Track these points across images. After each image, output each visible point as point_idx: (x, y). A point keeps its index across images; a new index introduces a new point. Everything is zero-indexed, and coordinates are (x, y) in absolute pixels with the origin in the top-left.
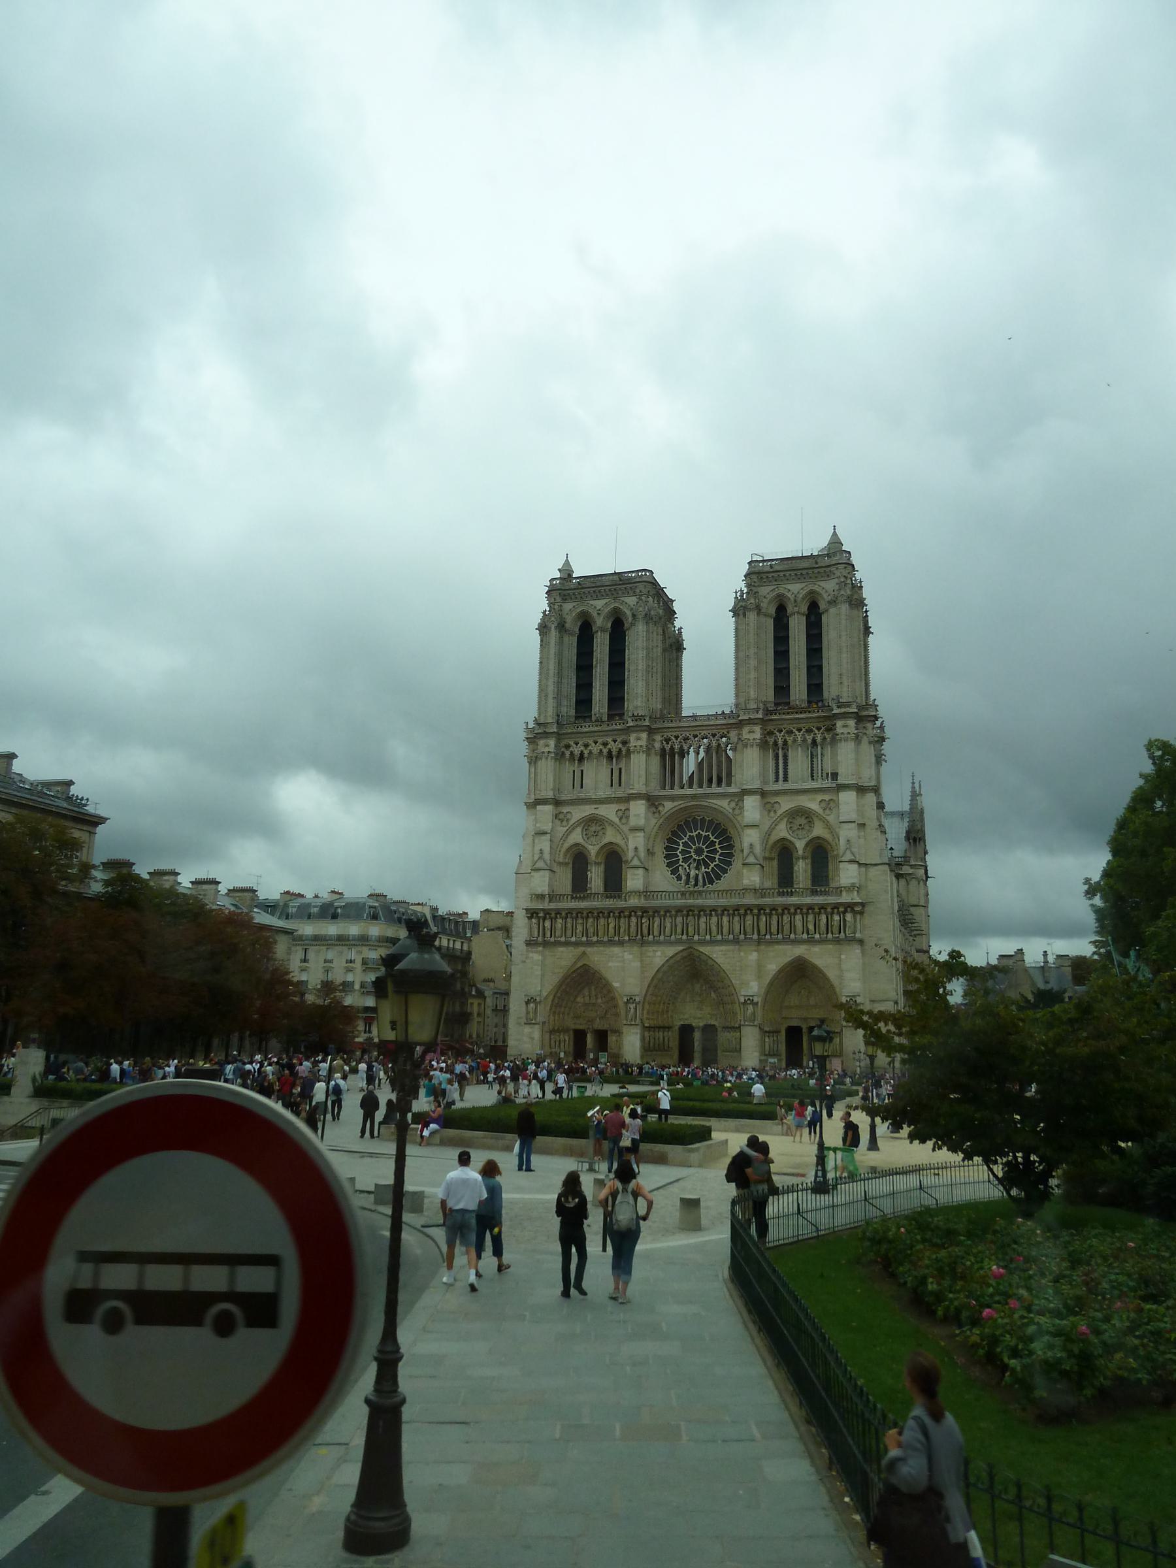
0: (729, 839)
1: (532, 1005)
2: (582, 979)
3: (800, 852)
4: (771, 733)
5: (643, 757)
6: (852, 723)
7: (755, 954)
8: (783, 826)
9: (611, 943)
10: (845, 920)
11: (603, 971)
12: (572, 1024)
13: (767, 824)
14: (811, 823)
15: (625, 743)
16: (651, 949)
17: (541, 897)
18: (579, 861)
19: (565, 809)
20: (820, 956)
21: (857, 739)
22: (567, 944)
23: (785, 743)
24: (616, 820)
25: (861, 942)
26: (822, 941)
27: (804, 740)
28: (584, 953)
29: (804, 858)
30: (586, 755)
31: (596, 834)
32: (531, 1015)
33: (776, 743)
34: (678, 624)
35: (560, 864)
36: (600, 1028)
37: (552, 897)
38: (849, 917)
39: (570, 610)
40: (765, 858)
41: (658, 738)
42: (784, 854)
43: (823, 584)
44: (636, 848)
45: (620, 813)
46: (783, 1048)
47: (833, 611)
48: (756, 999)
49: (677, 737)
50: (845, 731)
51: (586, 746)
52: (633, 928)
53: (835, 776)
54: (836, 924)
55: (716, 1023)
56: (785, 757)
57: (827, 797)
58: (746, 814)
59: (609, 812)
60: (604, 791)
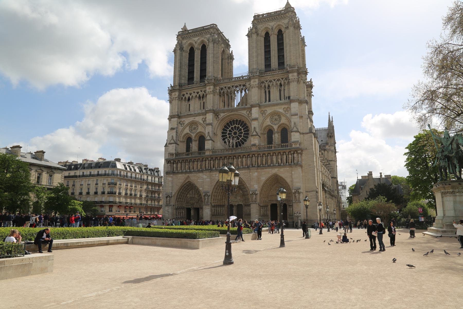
0: (247, 127)
1: (168, 198)
2: (188, 187)
3: (276, 130)
4: (263, 82)
5: (212, 95)
6: (295, 74)
7: (256, 173)
8: (268, 120)
9: (199, 171)
10: (294, 157)
11: (196, 183)
12: (185, 205)
13: (261, 119)
14: (280, 118)
15: (205, 91)
16: (214, 173)
17: (172, 154)
18: (189, 140)
19: (183, 120)
20: (283, 173)
21: (298, 82)
22: (182, 173)
23: (269, 86)
24: (202, 122)
25: (301, 166)
26: (285, 166)
27: (277, 84)
28: (188, 177)
29: (278, 133)
30: (190, 98)
31: (195, 129)
32: (168, 203)
33: (265, 87)
34: (231, 49)
35: (181, 141)
36: (196, 207)
37: (177, 154)
38: (295, 155)
39: (186, 43)
40: (261, 134)
41: (218, 88)
42: (270, 133)
43: (283, 21)
44: (209, 132)
45: (203, 120)
46: (269, 213)
47: (287, 31)
48: (256, 192)
49: (225, 87)
50: (293, 77)
51: (191, 94)
52: (207, 165)
53: (289, 97)
54: (290, 158)
55: (242, 204)
56: (269, 92)
57: (286, 106)
58: (252, 115)
59: (199, 119)
60: (198, 111)
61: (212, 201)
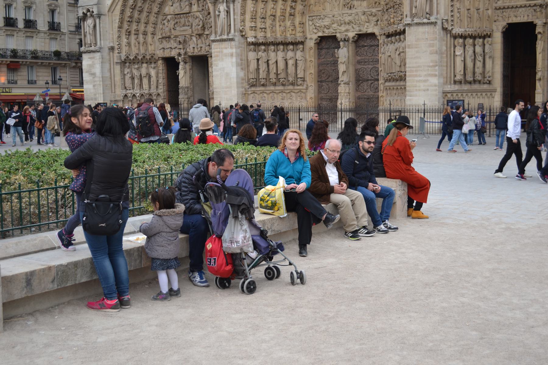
12: (159, 49)
36: (196, 52)
46: (496, 69)
55: (376, 31)
61: (248, 24)
